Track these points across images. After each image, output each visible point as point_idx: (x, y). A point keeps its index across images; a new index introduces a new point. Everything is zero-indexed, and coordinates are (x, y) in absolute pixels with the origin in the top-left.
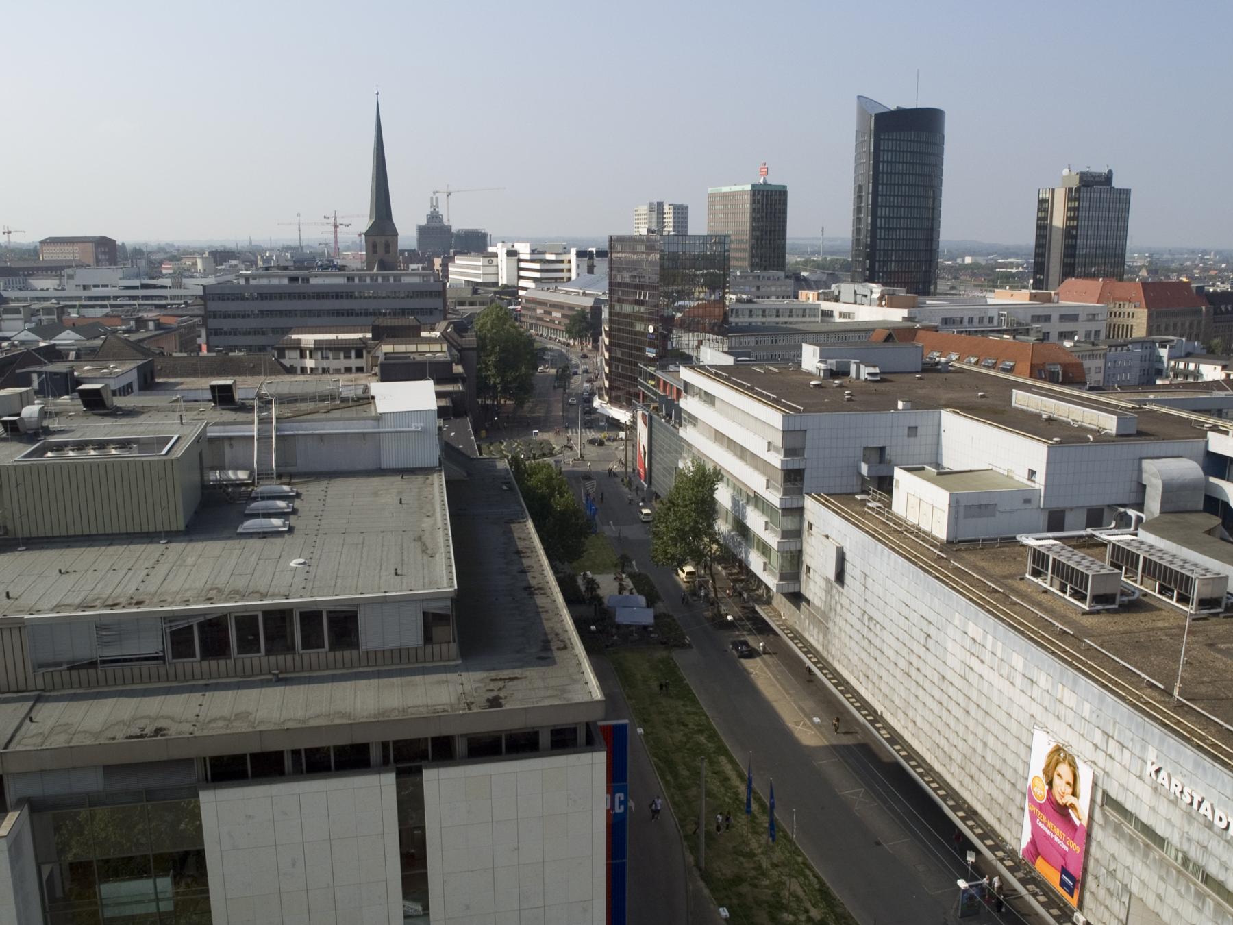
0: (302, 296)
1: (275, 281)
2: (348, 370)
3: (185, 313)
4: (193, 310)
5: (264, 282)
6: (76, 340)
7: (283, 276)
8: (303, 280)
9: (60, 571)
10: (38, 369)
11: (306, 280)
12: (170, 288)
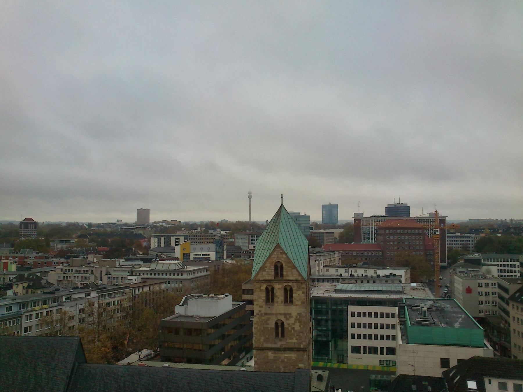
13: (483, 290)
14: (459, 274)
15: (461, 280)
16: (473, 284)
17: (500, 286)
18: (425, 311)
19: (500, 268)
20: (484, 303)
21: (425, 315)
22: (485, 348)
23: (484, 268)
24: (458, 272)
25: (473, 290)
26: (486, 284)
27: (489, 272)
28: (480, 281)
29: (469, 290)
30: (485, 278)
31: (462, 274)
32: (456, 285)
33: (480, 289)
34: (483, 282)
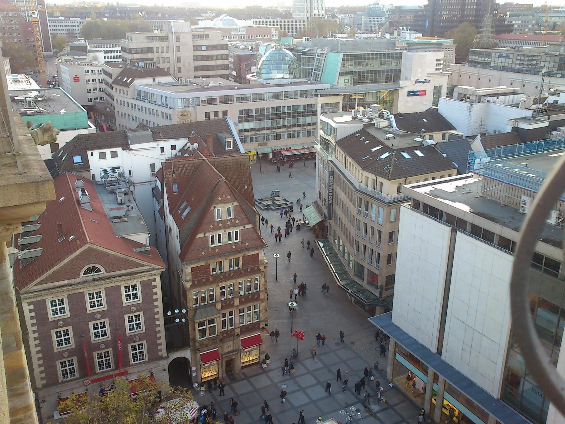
13: (90, 77)
14: (65, 62)
15: (67, 69)
16: (79, 71)
17: (105, 72)
18: (30, 101)
19: (106, 55)
20: (92, 90)
21: (30, 105)
22: (90, 128)
23: (92, 54)
24: (63, 61)
25: (80, 78)
26: (92, 71)
27: (96, 59)
28: (86, 68)
29: (76, 79)
30: (91, 65)
31: (68, 62)
32: (63, 75)
33: (87, 77)
34: (90, 69)
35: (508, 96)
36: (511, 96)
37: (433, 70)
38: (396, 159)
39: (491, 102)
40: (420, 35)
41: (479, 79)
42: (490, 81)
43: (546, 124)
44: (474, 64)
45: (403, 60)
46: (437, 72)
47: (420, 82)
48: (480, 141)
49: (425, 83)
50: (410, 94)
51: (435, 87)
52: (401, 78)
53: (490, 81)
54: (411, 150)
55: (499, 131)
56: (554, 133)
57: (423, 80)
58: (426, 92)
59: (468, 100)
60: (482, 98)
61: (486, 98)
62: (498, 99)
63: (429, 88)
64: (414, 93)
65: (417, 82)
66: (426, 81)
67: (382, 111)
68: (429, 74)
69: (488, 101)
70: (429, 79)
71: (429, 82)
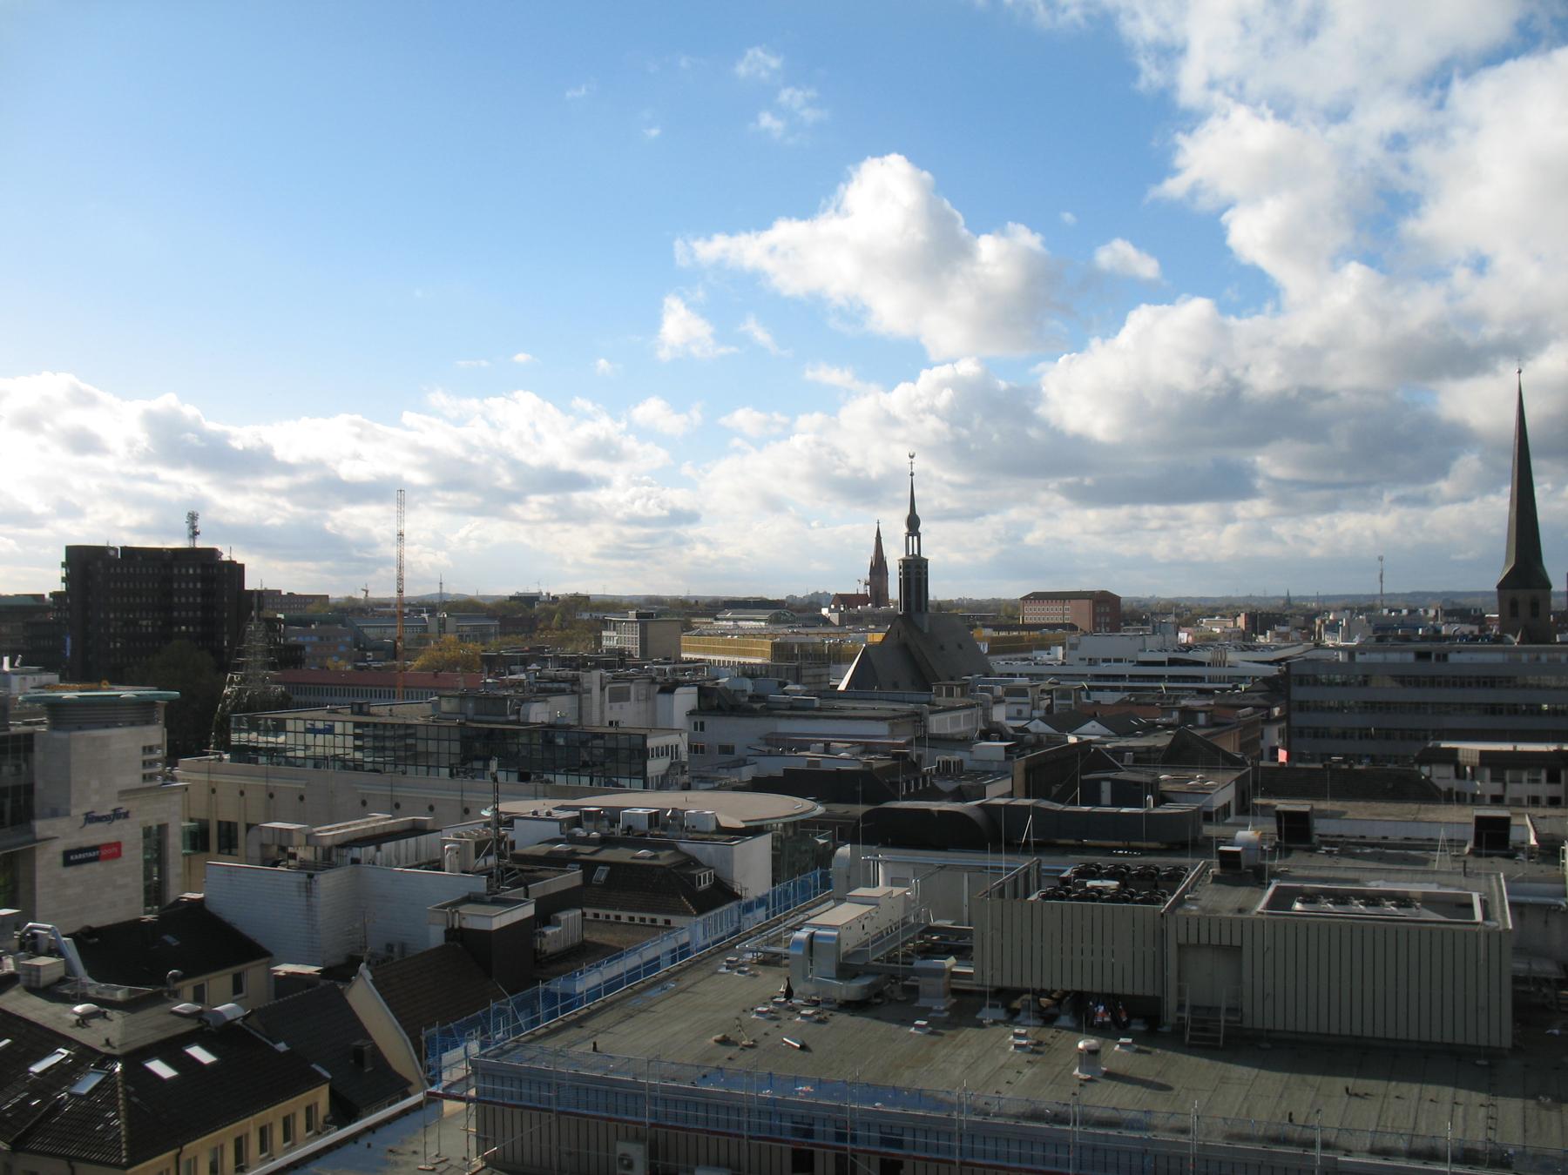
0: (1434, 682)
1: (1394, 657)
2: (1535, 801)
3: (1243, 702)
4: (1254, 698)
5: (1377, 657)
6: (1103, 736)
7: (1407, 651)
8: (1438, 657)
9: (1347, 1090)
10: (1111, 775)
11: (1443, 657)
12: (1209, 664)
35: (403, 842)
36: (412, 841)
37: (134, 780)
38: (132, 1089)
39: (363, 861)
40: (53, 678)
41: (271, 796)
42: (302, 798)
43: (528, 911)
44: (244, 754)
45: (38, 756)
46: (147, 785)
47: (99, 819)
48: (370, 983)
49: (117, 822)
50: (71, 858)
51: (147, 832)
52: (37, 811)
53: (302, 798)
54: (171, 1050)
55: (403, 947)
56: (549, 931)
57: (108, 812)
58: (120, 850)
59: (291, 862)
60: (334, 852)
61: (345, 851)
62: (379, 854)
63: (129, 834)
64: (80, 856)
65: (90, 818)
66: (118, 815)
67: (31, 928)
68: (123, 793)
69: (355, 861)
70: (125, 807)
71: (126, 815)
